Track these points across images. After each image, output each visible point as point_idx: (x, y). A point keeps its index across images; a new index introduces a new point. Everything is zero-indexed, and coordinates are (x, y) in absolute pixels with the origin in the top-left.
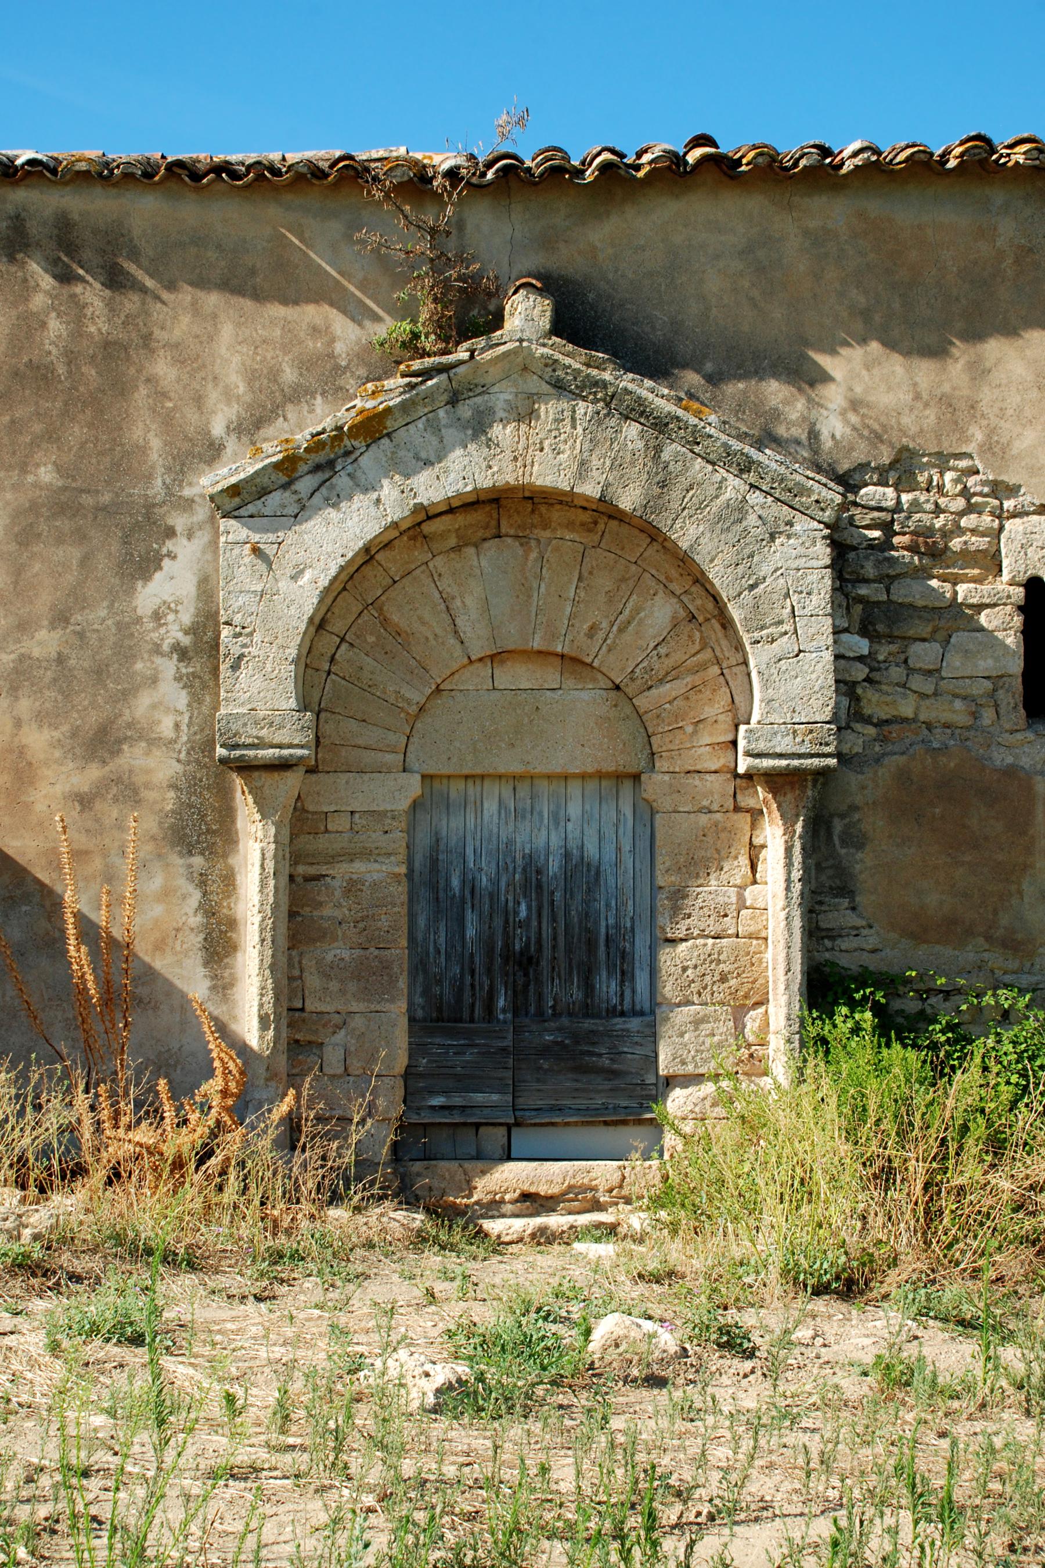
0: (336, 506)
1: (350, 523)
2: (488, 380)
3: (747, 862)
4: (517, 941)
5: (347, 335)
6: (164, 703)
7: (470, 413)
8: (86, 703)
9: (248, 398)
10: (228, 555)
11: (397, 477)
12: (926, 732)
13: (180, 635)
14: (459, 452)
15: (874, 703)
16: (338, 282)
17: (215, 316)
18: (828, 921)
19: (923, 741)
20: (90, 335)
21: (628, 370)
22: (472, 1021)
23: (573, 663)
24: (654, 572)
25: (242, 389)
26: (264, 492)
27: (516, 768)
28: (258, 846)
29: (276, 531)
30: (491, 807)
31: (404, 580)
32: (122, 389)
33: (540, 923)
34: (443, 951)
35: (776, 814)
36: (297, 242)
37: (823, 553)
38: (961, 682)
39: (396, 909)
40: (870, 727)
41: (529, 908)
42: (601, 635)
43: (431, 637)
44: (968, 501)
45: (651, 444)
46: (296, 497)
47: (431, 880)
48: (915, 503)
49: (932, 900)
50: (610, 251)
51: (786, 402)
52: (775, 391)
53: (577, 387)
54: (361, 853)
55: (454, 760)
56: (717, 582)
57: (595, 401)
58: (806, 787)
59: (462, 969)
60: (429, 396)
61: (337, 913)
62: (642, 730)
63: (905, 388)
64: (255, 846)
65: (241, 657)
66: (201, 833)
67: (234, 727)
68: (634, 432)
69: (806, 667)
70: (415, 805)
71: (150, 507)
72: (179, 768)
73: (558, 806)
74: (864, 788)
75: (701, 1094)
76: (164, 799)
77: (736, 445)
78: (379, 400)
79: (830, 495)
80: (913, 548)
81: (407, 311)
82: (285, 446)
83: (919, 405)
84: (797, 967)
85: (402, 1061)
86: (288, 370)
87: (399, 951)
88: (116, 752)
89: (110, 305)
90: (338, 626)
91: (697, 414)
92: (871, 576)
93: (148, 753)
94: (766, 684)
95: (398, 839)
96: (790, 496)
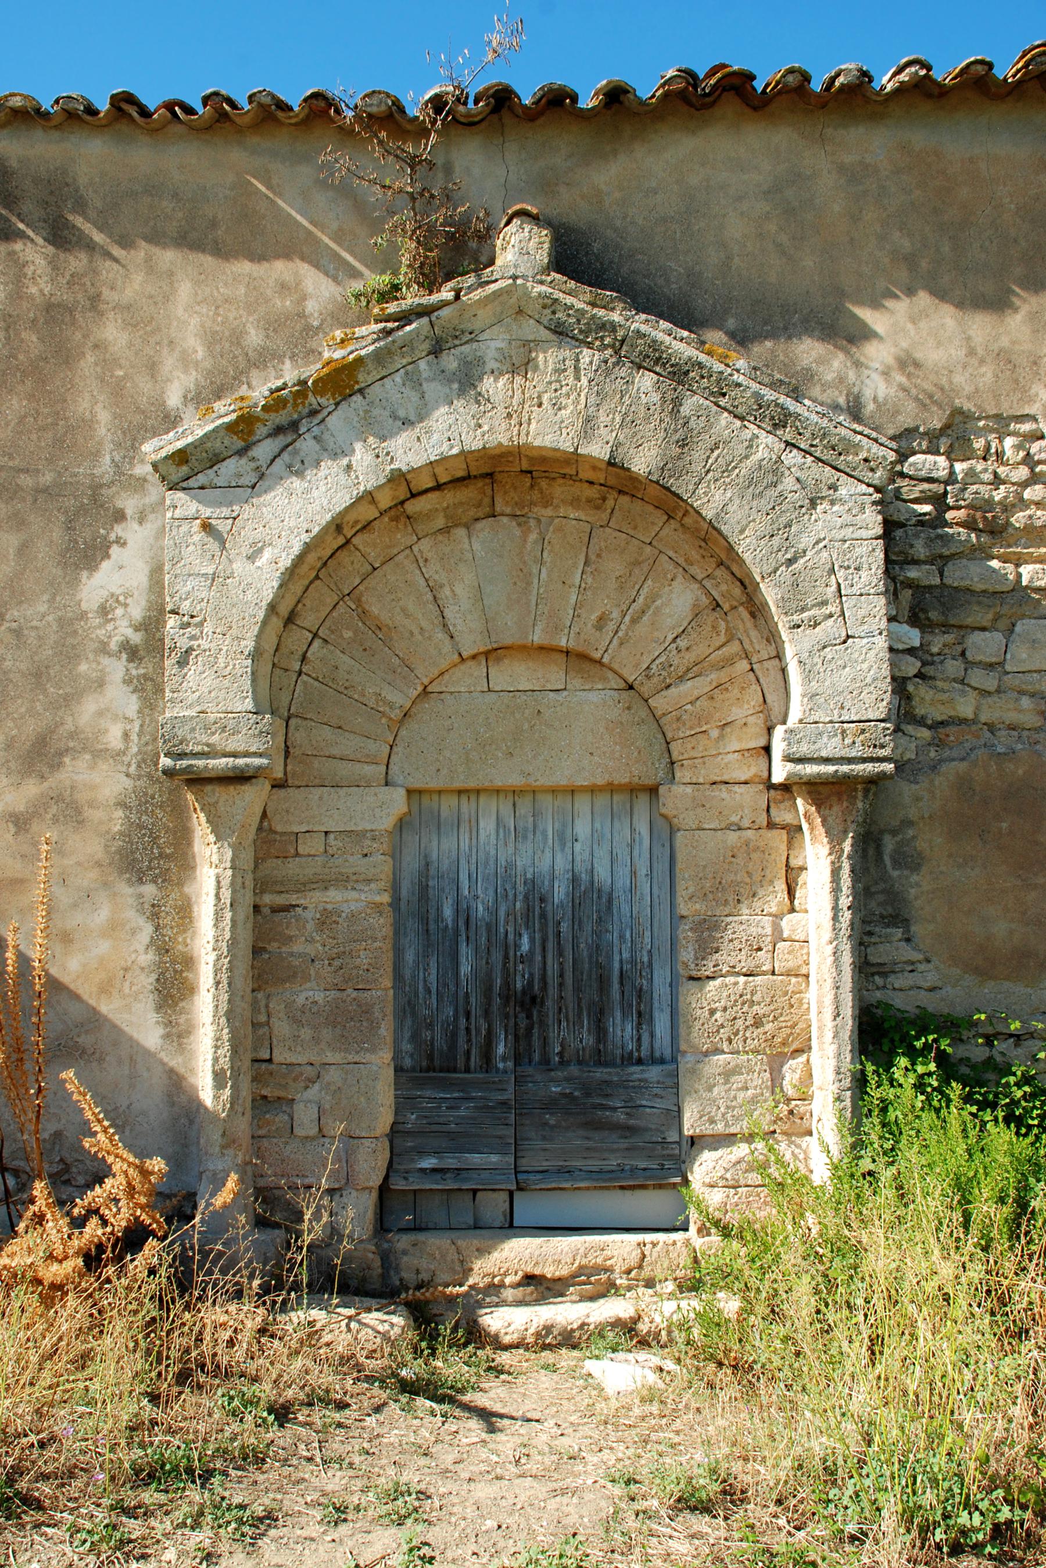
0: (300, 474)
1: (315, 493)
2: (477, 325)
3: (784, 887)
4: (518, 978)
5: (319, 292)
6: (110, 711)
7: (455, 364)
8: (23, 710)
9: (207, 364)
10: (174, 533)
11: (371, 440)
12: (988, 735)
13: (129, 632)
14: (444, 410)
15: (928, 702)
16: (310, 233)
17: (171, 274)
18: (878, 954)
19: (985, 745)
20: (31, 297)
21: (639, 311)
22: (467, 1070)
23: (579, 660)
24: (671, 554)
25: (200, 355)
26: (216, 460)
27: (515, 780)
28: (213, 872)
29: (231, 504)
30: (487, 826)
31: (385, 567)
32: (65, 356)
33: (544, 957)
34: (434, 990)
35: (821, 830)
36: (263, 189)
37: (872, 521)
38: (1028, 676)
39: (377, 944)
40: (924, 729)
41: (532, 940)
42: (611, 626)
43: (416, 632)
44: (1032, 470)
45: (669, 396)
46: (253, 465)
47: (421, 912)
48: (971, 473)
49: (1001, 928)
50: (617, 195)
51: (821, 361)
52: (808, 351)
53: (581, 331)
54: (336, 880)
55: (444, 772)
56: (747, 557)
57: (603, 348)
58: (855, 797)
59: (456, 1011)
60: (406, 345)
61: (310, 950)
62: (660, 736)
63: (957, 343)
64: (211, 869)
65: (189, 651)
66: (152, 858)
67: (179, 733)
68: (649, 383)
69: (856, 655)
70: (402, 824)
71: (96, 488)
72: (128, 783)
73: (564, 825)
74: (918, 799)
75: (733, 1158)
76: (111, 820)
77: (769, 395)
78: (349, 349)
79: (882, 452)
80: (969, 525)
81: (386, 262)
82: (240, 405)
83: (974, 361)
84: (848, 1011)
85: (385, 1119)
86: (253, 332)
87: (382, 991)
88: (56, 766)
89: (54, 265)
90: (309, 619)
91: (723, 359)
92: (922, 557)
93: (92, 767)
94: (808, 676)
95: (381, 866)
96: (833, 454)
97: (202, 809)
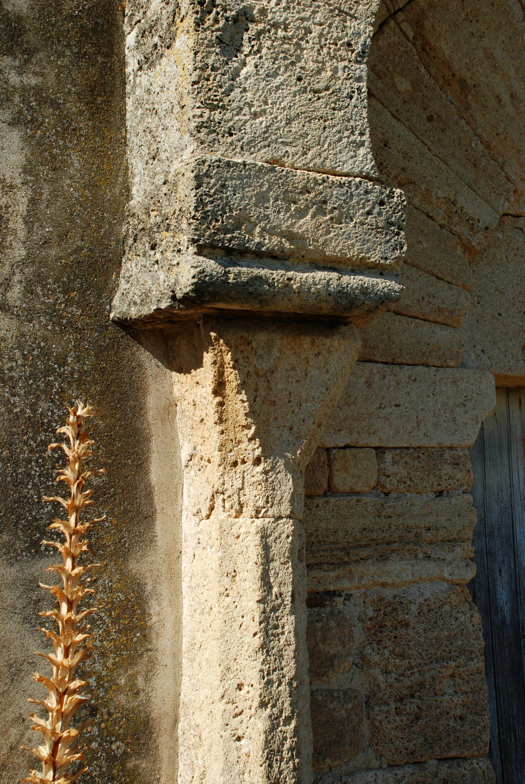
43: (506, 98)
61: (359, 683)
67: (235, 201)
97: (242, 386)
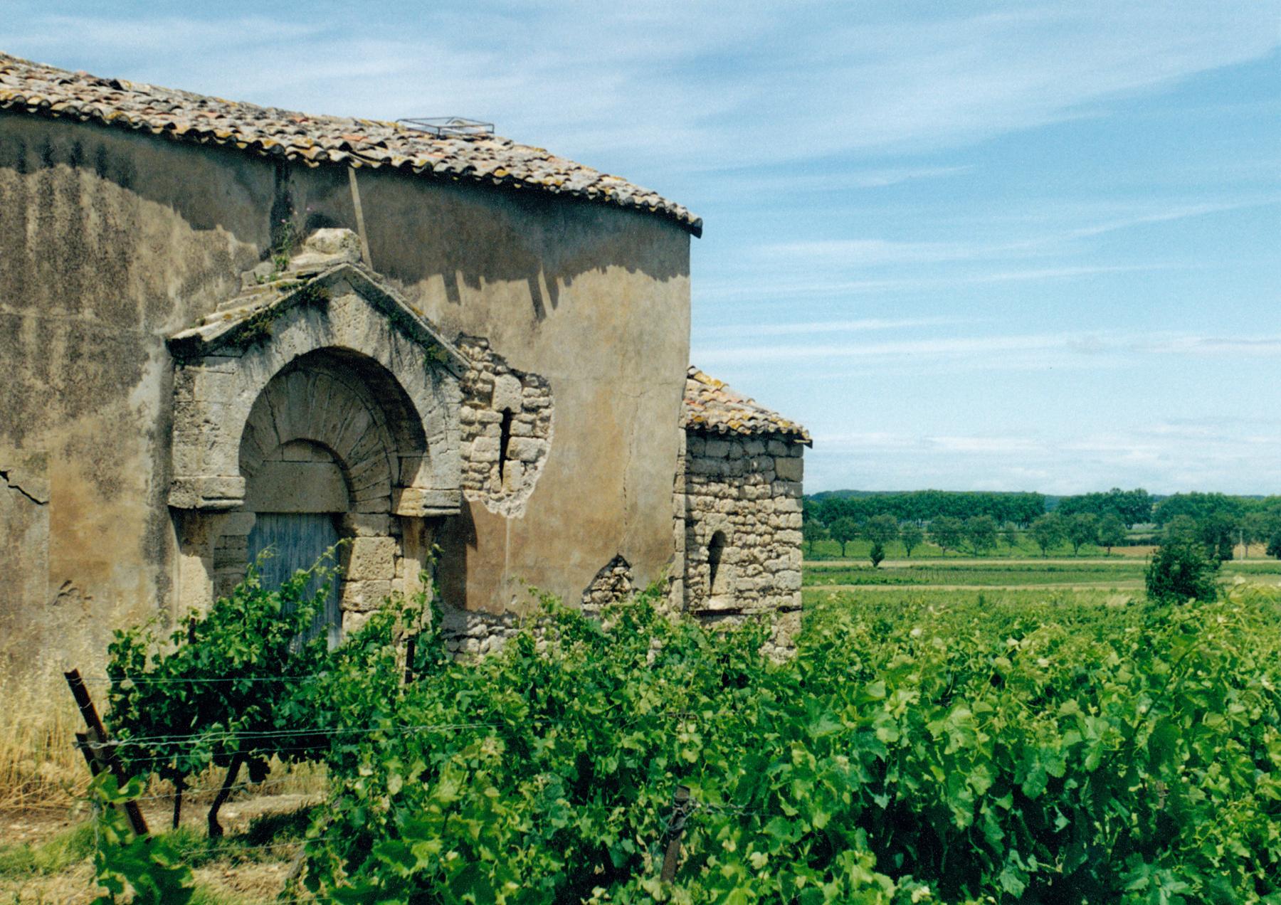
23: (319, 447)
25: (184, 269)
27: (294, 509)
72: (148, 508)
